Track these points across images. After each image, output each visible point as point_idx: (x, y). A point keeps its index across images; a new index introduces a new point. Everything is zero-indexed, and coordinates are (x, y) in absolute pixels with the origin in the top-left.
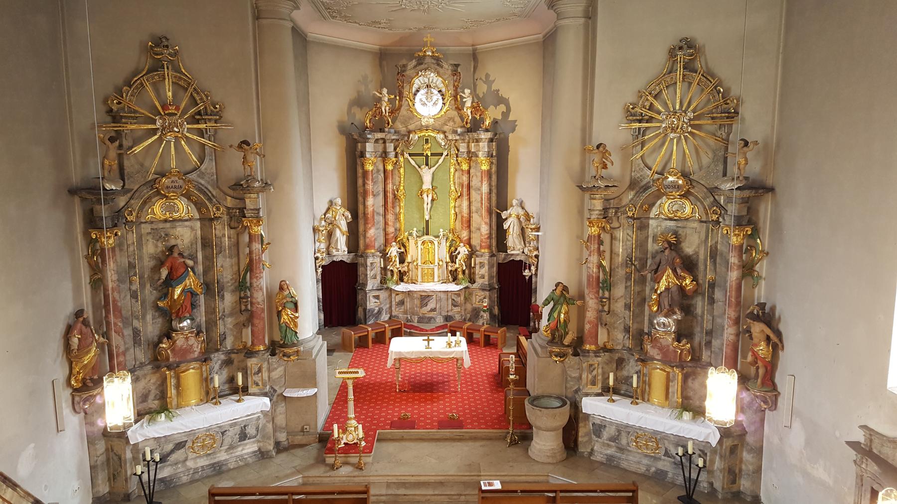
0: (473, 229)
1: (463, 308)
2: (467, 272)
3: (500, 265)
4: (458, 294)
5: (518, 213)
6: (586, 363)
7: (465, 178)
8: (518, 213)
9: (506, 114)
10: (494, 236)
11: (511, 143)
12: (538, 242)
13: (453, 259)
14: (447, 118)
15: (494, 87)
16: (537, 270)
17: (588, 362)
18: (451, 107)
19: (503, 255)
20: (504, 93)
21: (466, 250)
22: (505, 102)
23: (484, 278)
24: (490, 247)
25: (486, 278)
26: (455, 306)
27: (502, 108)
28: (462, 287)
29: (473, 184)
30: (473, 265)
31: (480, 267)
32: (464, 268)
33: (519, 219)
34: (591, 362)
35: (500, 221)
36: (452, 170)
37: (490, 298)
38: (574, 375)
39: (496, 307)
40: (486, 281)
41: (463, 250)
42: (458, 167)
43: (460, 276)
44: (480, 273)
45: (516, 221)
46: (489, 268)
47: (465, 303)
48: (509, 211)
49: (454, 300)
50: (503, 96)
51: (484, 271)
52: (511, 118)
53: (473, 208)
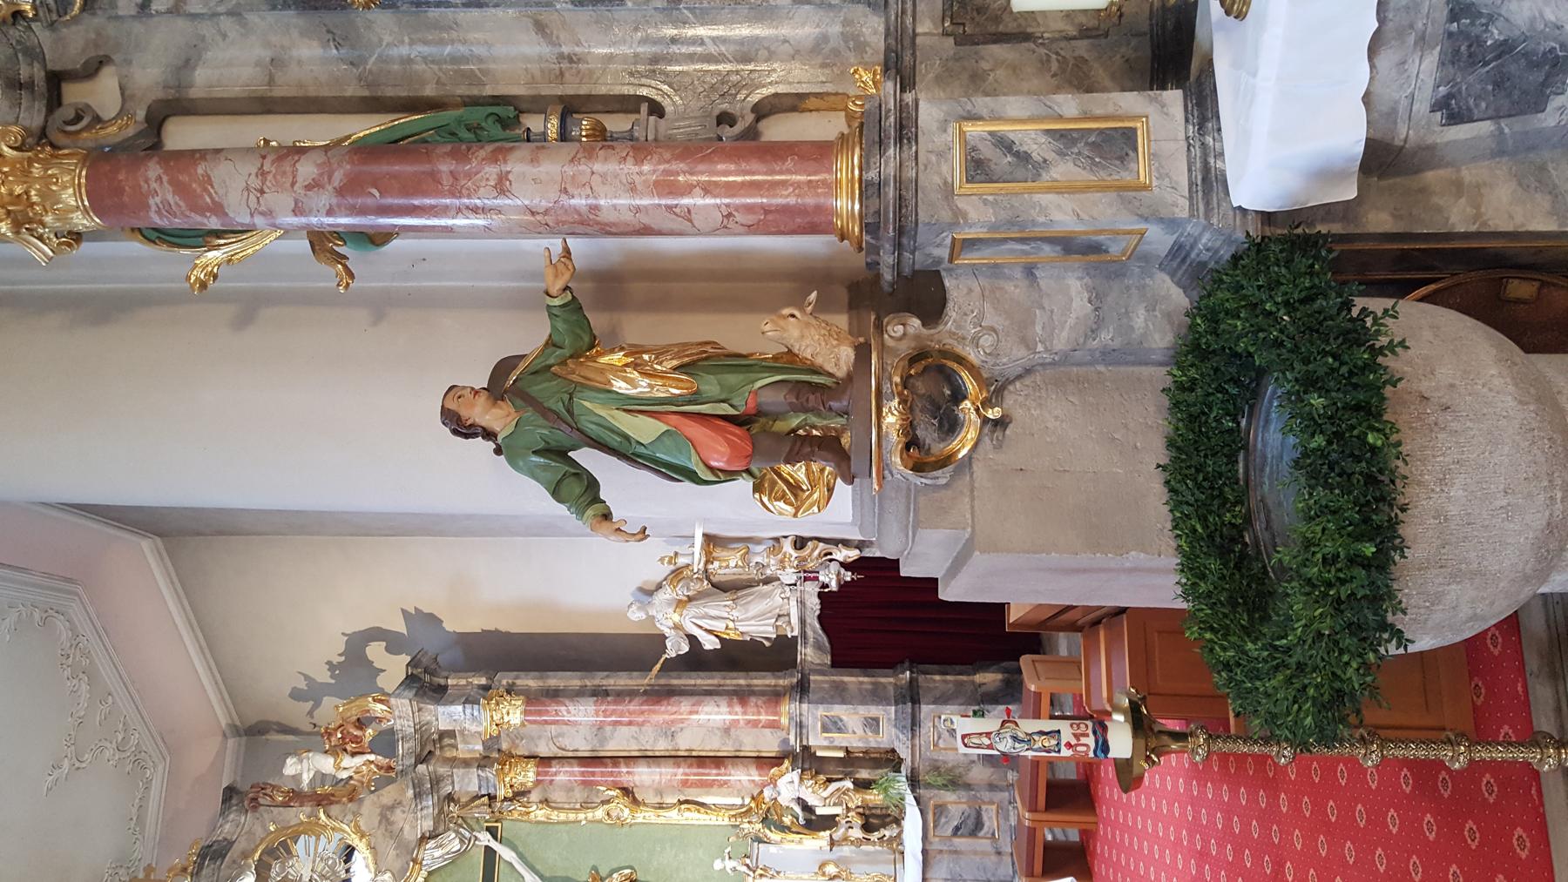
0: (727, 749)
1: (986, 795)
2: (864, 774)
3: (841, 661)
4: (932, 816)
5: (669, 603)
6: (961, 203)
7: (564, 775)
8: (669, 603)
9: (394, 643)
10: (742, 682)
11: (474, 625)
12: (758, 541)
13: (815, 823)
14: (383, 827)
15: (324, 676)
16: (846, 543)
17: (948, 190)
18: (350, 817)
19: (809, 654)
20: (334, 649)
21: (788, 777)
22: (357, 644)
23: (876, 720)
24: (775, 696)
25: (874, 711)
26: (979, 824)
27: (376, 651)
28: (910, 799)
29: (584, 748)
30: (841, 754)
31: (840, 730)
32: (848, 784)
33: (690, 599)
34: (955, 167)
35: (696, 659)
36: (539, 814)
37: (942, 699)
38: (1080, 305)
39: (979, 678)
40: (886, 713)
41: (789, 787)
42: (534, 797)
43: (874, 797)
44: (860, 732)
45: (692, 610)
46: (844, 702)
47: (968, 787)
48: (667, 632)
49: (957, 829)
50: (342, 649)
51: (852, 716)
52: (400, 627)
53: (662, 746)
